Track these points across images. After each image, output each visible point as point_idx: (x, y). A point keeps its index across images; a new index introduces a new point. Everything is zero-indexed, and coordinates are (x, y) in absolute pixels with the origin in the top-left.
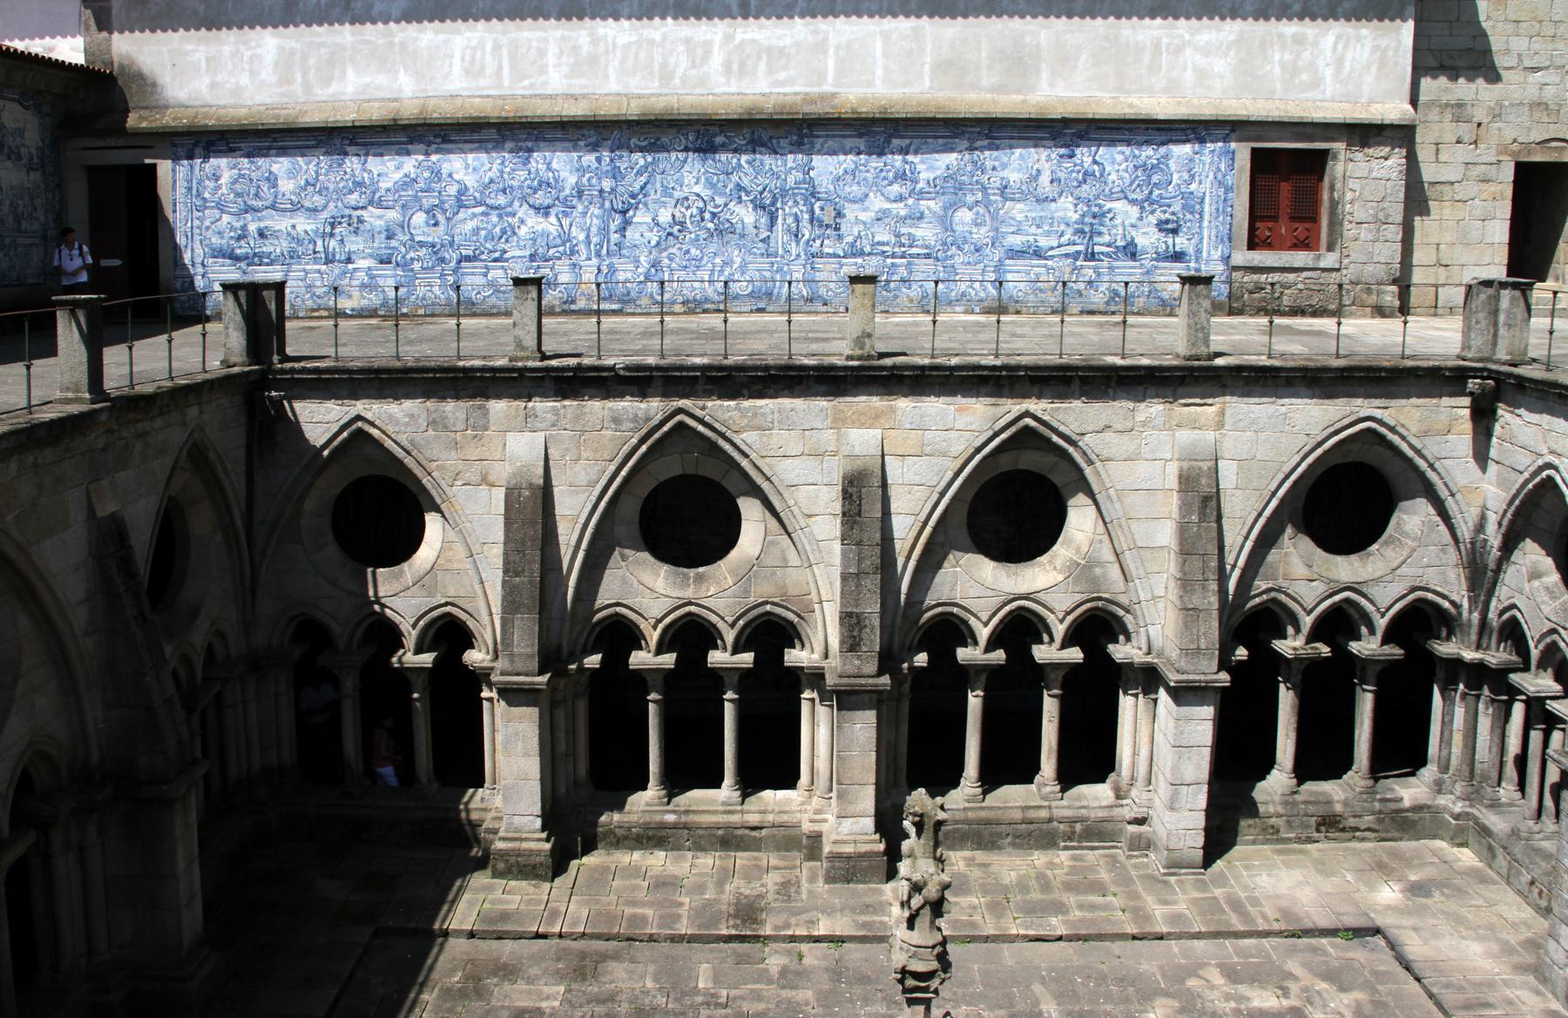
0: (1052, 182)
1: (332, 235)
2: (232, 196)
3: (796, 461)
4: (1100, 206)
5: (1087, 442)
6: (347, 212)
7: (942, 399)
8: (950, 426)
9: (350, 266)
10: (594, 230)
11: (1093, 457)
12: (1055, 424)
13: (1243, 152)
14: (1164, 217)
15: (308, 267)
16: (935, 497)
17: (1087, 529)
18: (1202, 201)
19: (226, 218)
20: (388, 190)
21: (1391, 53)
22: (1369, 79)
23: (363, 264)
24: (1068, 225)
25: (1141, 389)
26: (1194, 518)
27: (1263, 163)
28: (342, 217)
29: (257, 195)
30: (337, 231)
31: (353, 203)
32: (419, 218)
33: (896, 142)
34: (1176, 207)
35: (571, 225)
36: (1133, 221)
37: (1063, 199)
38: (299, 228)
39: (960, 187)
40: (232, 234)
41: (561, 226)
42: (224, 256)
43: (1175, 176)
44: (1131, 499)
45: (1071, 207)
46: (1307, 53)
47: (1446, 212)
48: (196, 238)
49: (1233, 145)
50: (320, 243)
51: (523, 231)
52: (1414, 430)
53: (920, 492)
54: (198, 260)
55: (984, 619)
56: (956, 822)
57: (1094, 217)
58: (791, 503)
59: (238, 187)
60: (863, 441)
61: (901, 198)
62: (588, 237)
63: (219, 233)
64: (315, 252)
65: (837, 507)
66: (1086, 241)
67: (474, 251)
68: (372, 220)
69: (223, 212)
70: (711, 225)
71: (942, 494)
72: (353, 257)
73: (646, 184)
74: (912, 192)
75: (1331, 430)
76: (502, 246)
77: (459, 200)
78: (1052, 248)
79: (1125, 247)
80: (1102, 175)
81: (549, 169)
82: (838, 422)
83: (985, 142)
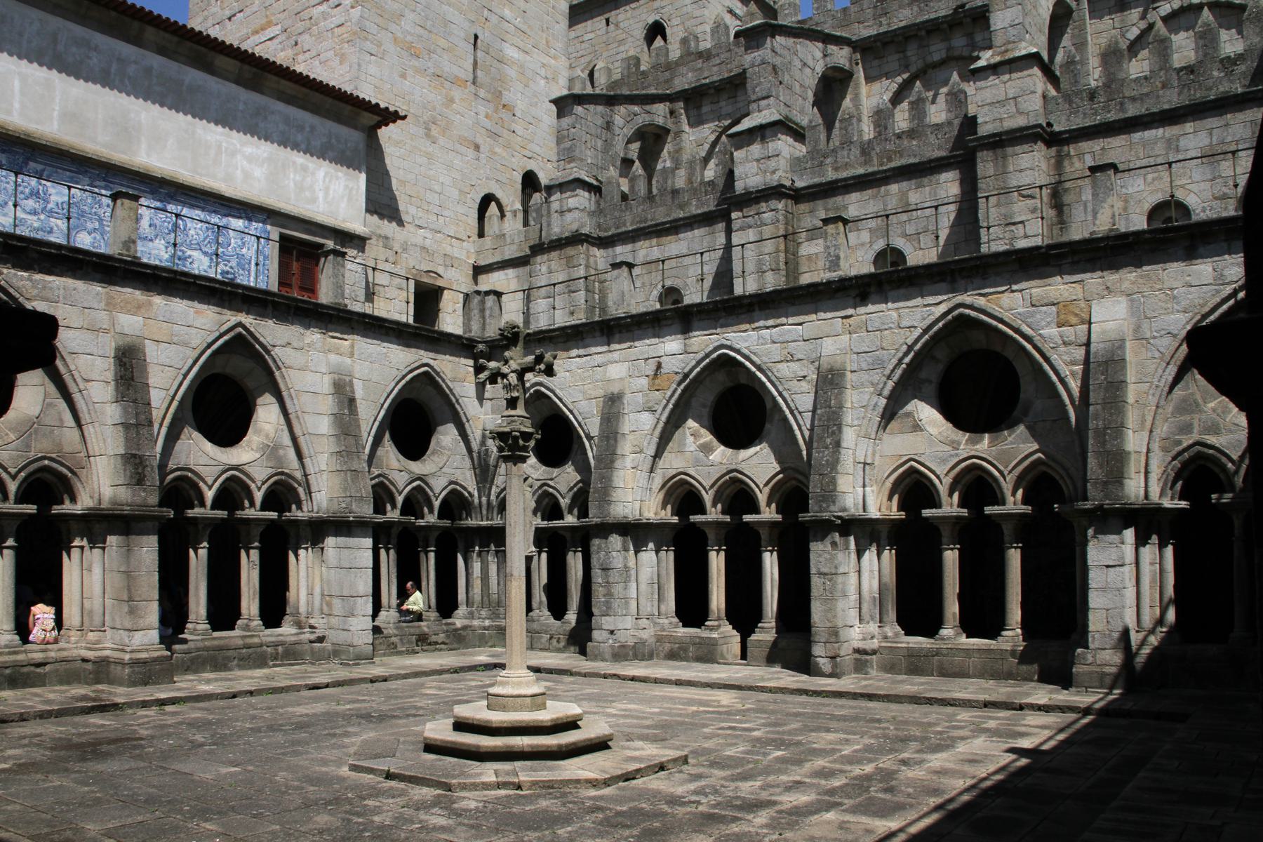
0: (150, 226)
3: (77, 333)
4: (184, 252)
5: (277, 352)
7: (185, 302)
8: (190, 324)
11: (280, 364)
12: (258, 335)
13: (275, 233)
14: (227, 268)
16: (181, 377)
17: (272, 421)
18: (250, 261)
21: (354, 192)
22: (343, 205)
25: (307, 320)
26: (346, 411)
27: (287, 245)
33: (32, 165)
34: (234, 263)
37: (157, 241)
39: (82, 215)
43: (233, 241)
44: (305, 398)
45: (163, 248)
46: (309, 179)
47: (382, 304)
49: (269, 227)
52: (449, 376)
53: (170, 373)
55: (210, 483)
56: (198, 649)
57: (179, 259)
58: (72, 367)
60: (130, 323)
61: (34, 213)
65: (110, 375)
71: (185, 376)
74: (44, 209)
75: (409, 368)
82: (110, 306)
83: (103, 184)
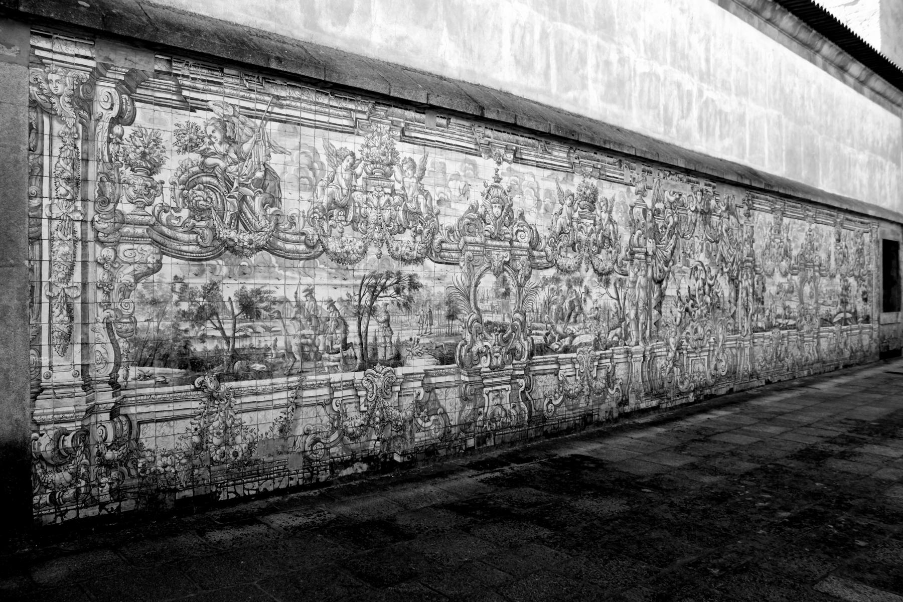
1: (372, 311)
2: (185, 213)
6: (395, 266)
9: (400, 371)
10: (641, 305)
15: (335, 377)
19: (171, 267)
20: (451, 231)
23: (418, 365)
28: (388, 275)
29: (238, 216)
30: (380, 303)
31: (404, 250)
32: (488, 282)
35: (625, 298)
38: (321, 294)
40: (185, 306)
41: (618, 299)
42: (166, 361)
48: (99, 314)
50: (353, 326)
51: (588, 307)
54: (102, 372)
59: (199, 195)
62: (637, 315)
63: (154, 302)
64: (346, 346)
67: (545, 338)
68: (430, 283)
69: (163, 249)
70: (708, 300)
72: (404, 353)
73: (674, 248)
76: (572, 328)
77: (531, 257)
81: (610, 220)
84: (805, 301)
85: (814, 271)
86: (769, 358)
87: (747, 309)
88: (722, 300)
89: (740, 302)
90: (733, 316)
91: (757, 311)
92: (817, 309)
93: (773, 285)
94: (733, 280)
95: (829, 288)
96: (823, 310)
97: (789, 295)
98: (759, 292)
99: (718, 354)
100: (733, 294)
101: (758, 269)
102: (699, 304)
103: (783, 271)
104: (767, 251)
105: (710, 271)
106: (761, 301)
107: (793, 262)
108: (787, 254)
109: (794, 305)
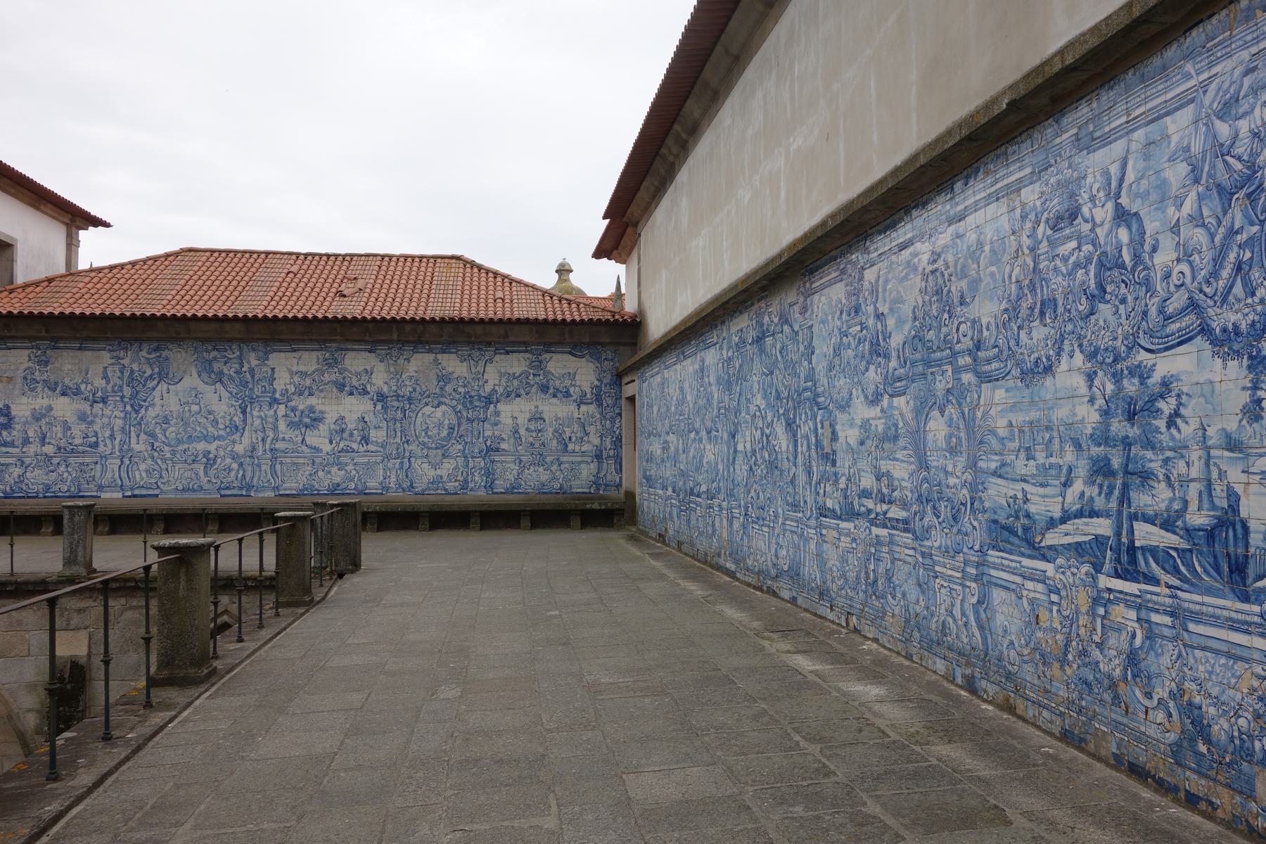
24: (1078, 446)
36: (1232, 425)
66: (1113, 505)
78: (1052, 523)
79: (1211, 534)
80: (1137, 258)
84: (935, 460)
85: (957, 371)
86: (852, 575)
87: (809, 473)
88: (779, 457)
89: (800, 459)
90: (792, 482)
91: (824, 478)
92: (975, 488)
93: (852, 425)
94: (791, 426)
95: (1018, 418)
96: (998, 493)
97: (887, 446)
98: (826, 443)
99: (778, 535)
100: (791, 448)
101: (821, 399)
102: (760, 462)
103: (871, 389)
104: (837, 361)
105: (766, 417)
106: (830, 458)
107: (893, 363)
108: (878, 350)
109: (901, 471)
